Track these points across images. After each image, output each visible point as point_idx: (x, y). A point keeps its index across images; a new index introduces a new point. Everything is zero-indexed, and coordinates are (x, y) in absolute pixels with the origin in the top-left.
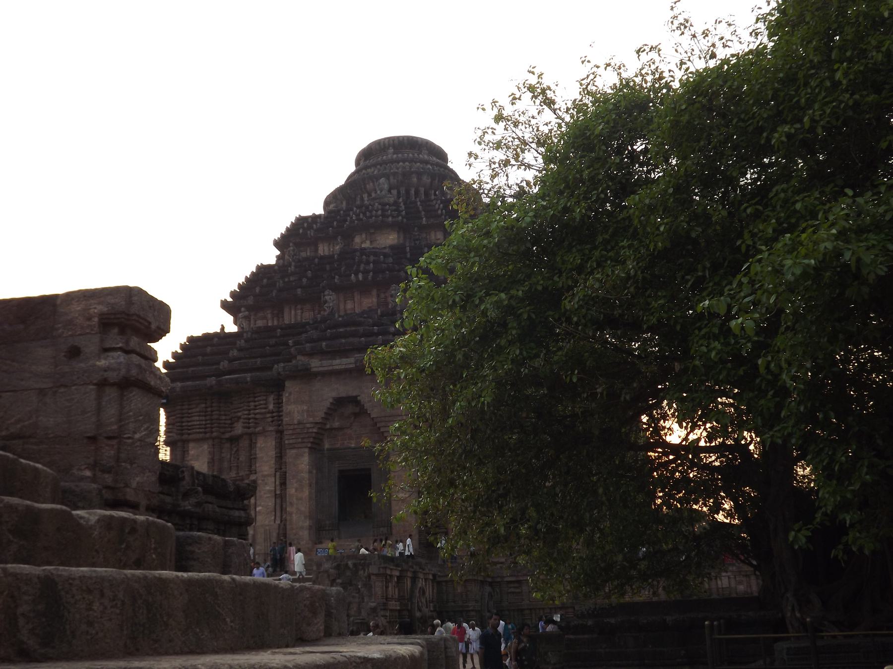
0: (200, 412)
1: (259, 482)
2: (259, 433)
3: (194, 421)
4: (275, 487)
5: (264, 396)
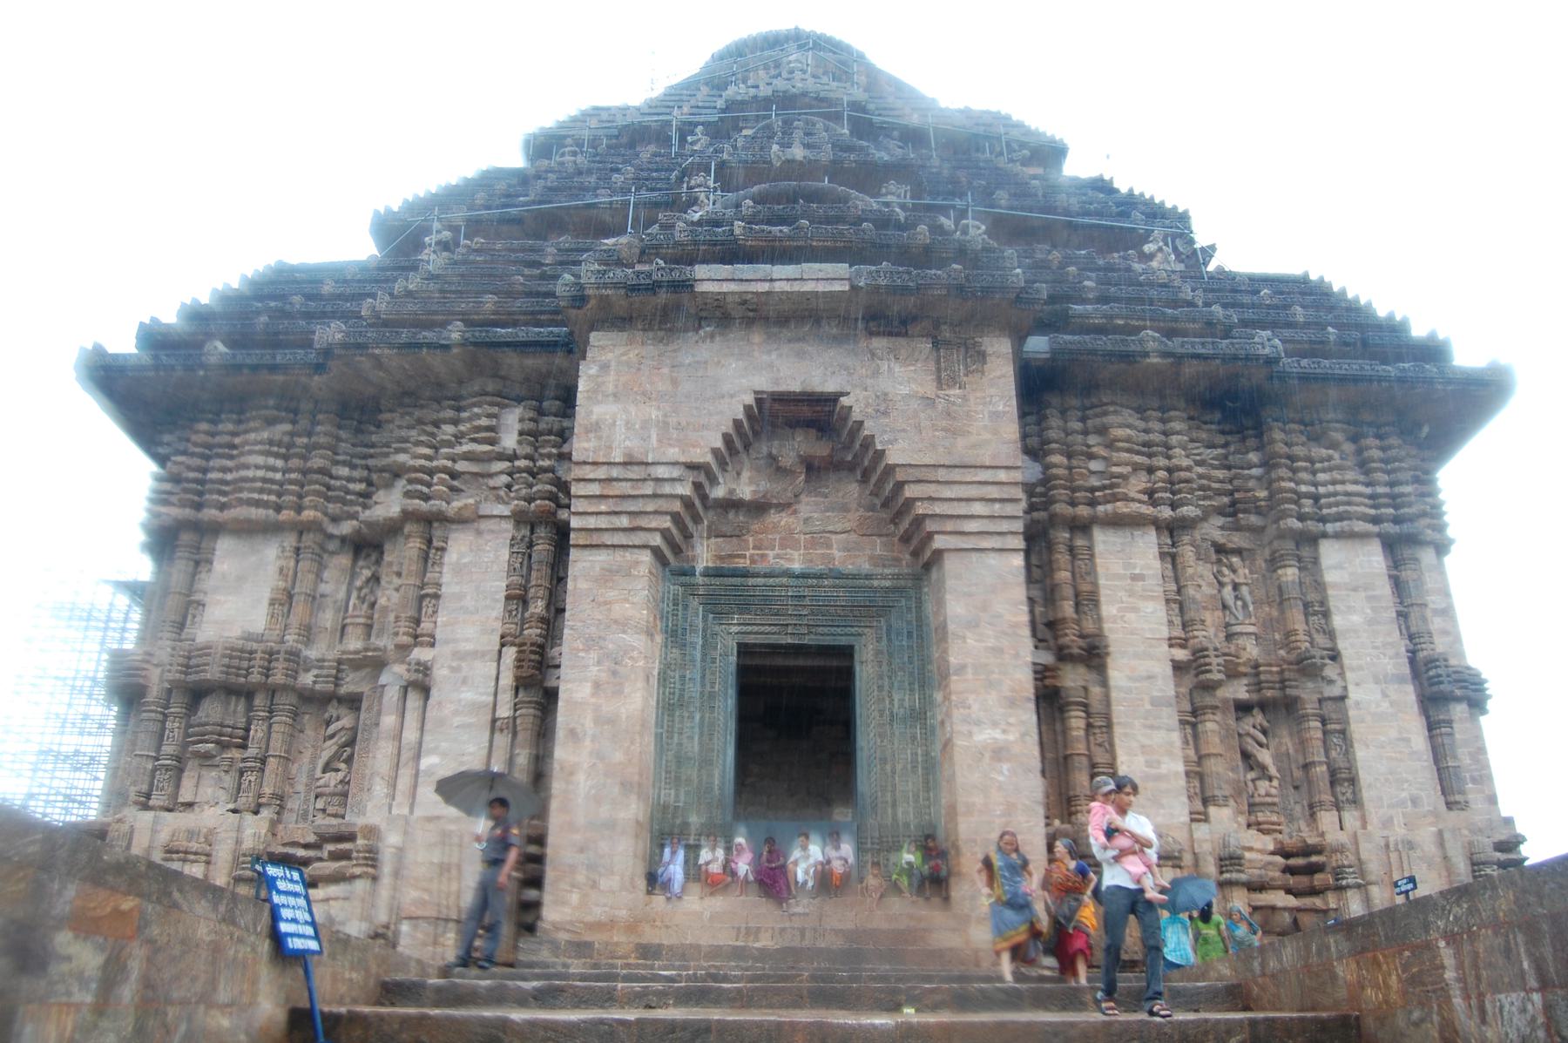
0: (271, 442)
1: (440, 673)
2: (461, 520)
3: (247, 467)
4: (496, 694)
5: (492, 404)
